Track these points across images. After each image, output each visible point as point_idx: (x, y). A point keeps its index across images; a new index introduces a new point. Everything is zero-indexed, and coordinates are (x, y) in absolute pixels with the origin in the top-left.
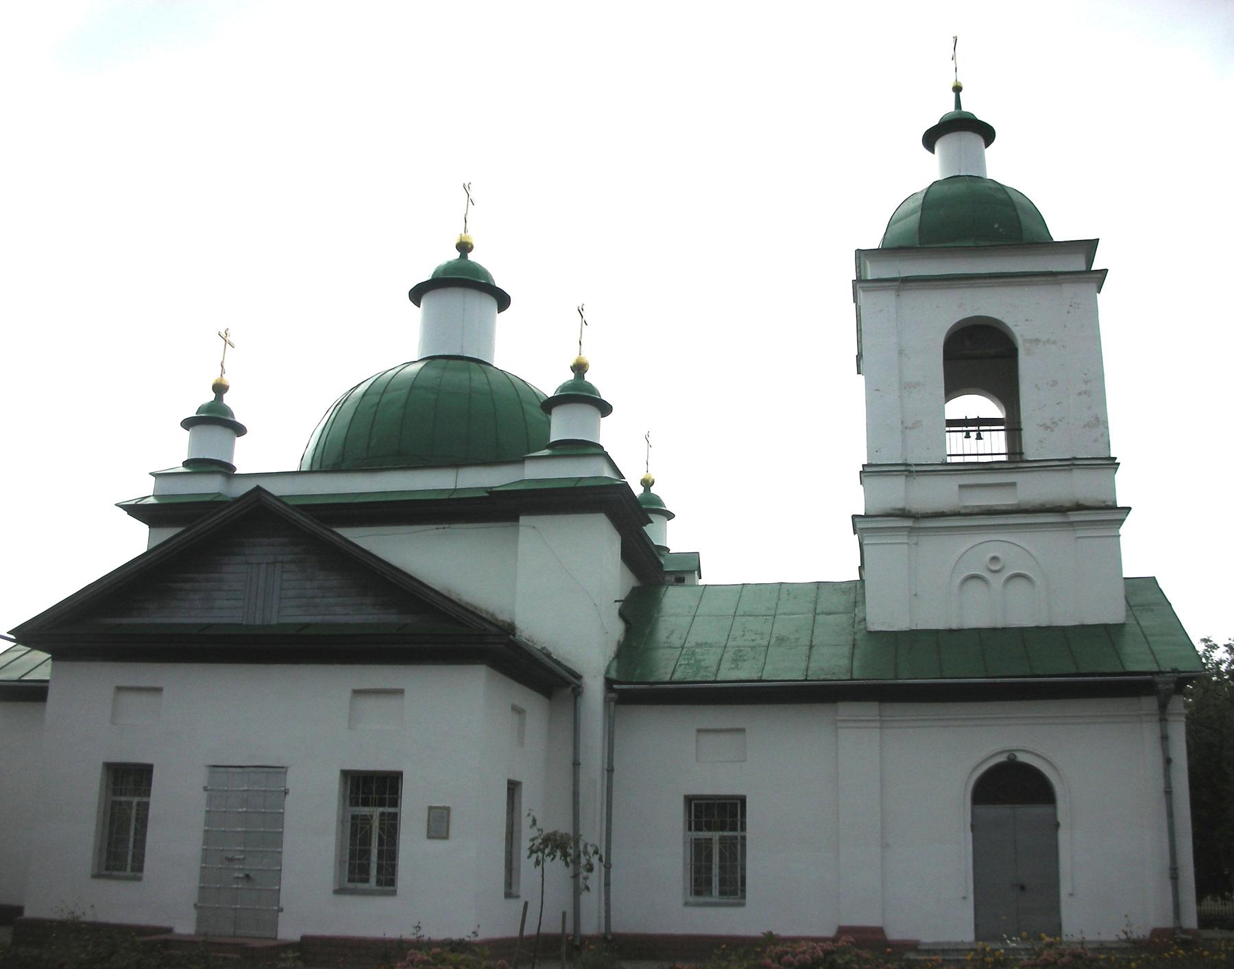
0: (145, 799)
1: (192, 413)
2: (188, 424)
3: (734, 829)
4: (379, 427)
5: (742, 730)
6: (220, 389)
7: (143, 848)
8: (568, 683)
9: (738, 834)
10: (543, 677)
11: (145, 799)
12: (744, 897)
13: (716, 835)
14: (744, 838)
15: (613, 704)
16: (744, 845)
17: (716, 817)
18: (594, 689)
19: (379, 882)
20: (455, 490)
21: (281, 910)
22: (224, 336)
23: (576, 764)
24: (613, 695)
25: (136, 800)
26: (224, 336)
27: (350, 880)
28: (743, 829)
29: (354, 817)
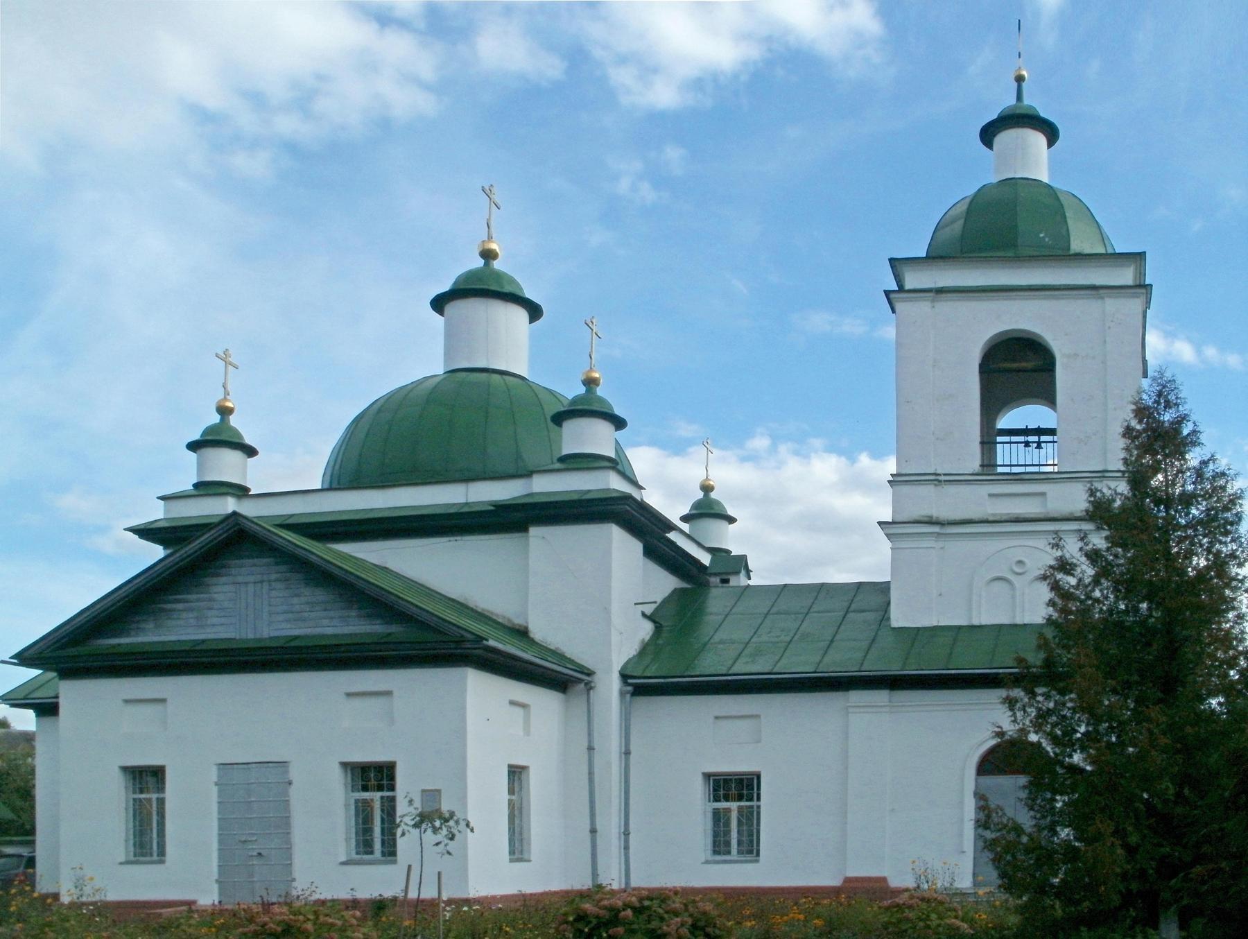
0: (161, 796)
1: (196, 436)
2: (194, 446)
3: (751, 799)
4: (393, 441)
5: (758, 716)
6: (224, 412)
7: (164, 836)
8: (580, 680)
9: (754, 803)
10: (560, 677)
11: (161, 796)
12: (758, 854)
13: (734, 805)
14: (759, 807)
15: (628, 696)
16: (759, 813)
17: (735, 789)
18: (610, 687)
19: (383, 854)
20: (467, 504)
21: (294, 880)
22: (225, 358)
23: (591, 749)
24: (630, 688)
25: (154, 796)
26: (225, 358)
27: (357, 853)
28: (759, 799)
29: (357, 801)
